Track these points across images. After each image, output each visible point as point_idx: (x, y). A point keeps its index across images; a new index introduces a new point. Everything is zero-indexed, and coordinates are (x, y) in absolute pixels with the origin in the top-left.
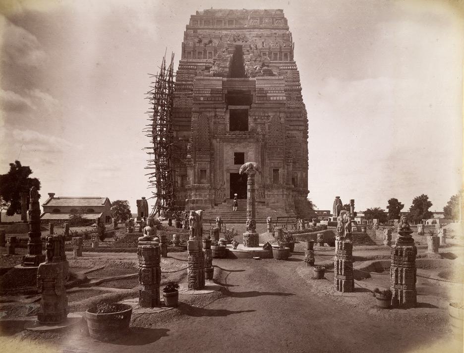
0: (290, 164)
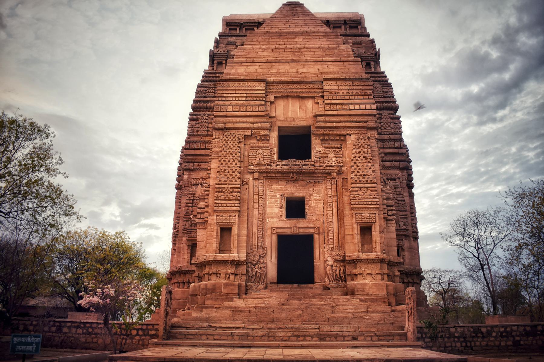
0: (391, 217)
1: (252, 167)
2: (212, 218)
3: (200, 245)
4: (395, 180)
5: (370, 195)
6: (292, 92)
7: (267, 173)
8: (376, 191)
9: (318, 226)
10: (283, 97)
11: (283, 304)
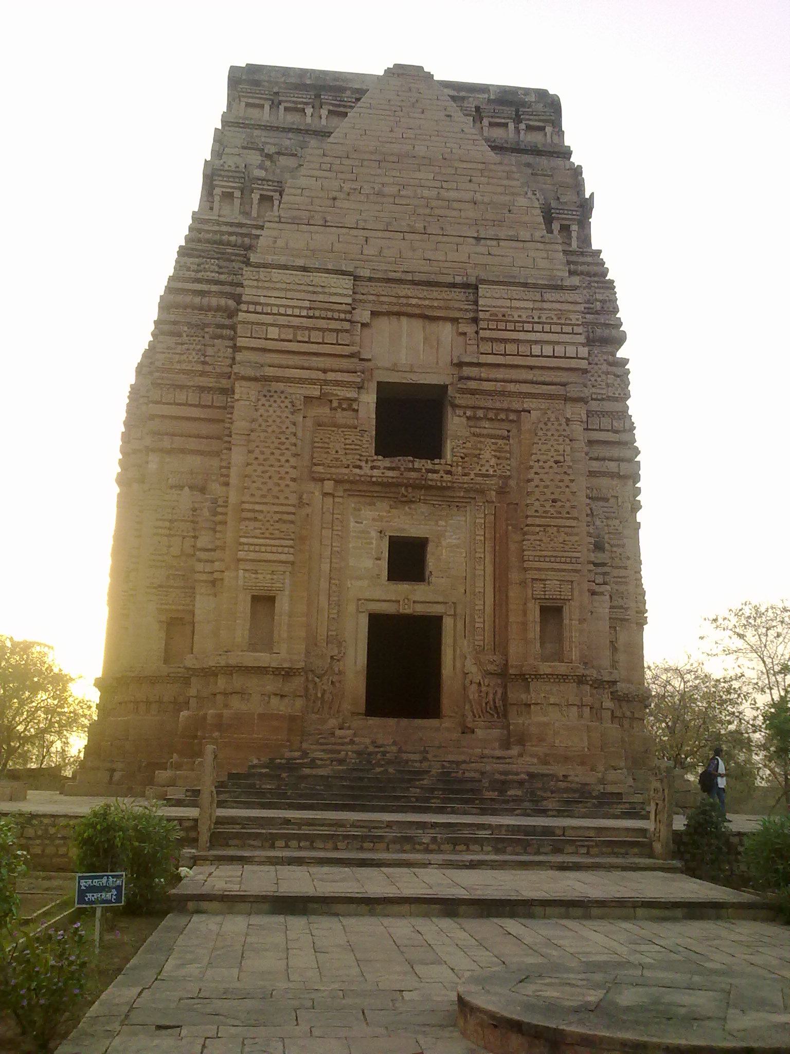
4: (607, 500)
6: (410, 305)
7: (352, 482)
9: (454, 600)
10: (389, 314)
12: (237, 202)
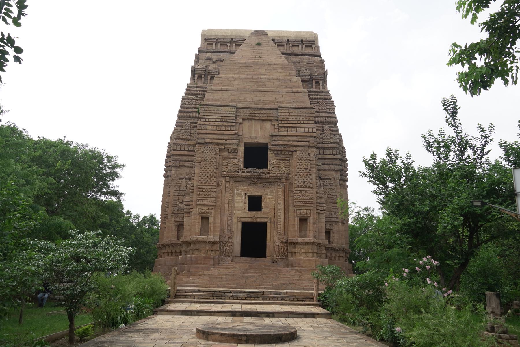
0: (323, 212)
1: (225, 173)
2: (196, 209)
3: (186, 227)
4: (330, 179)
5: (308, 196)
7: (235, 177)
8: (312, 193)
10: (248, 119)
11: (244, 273)
12: (203, 79)
